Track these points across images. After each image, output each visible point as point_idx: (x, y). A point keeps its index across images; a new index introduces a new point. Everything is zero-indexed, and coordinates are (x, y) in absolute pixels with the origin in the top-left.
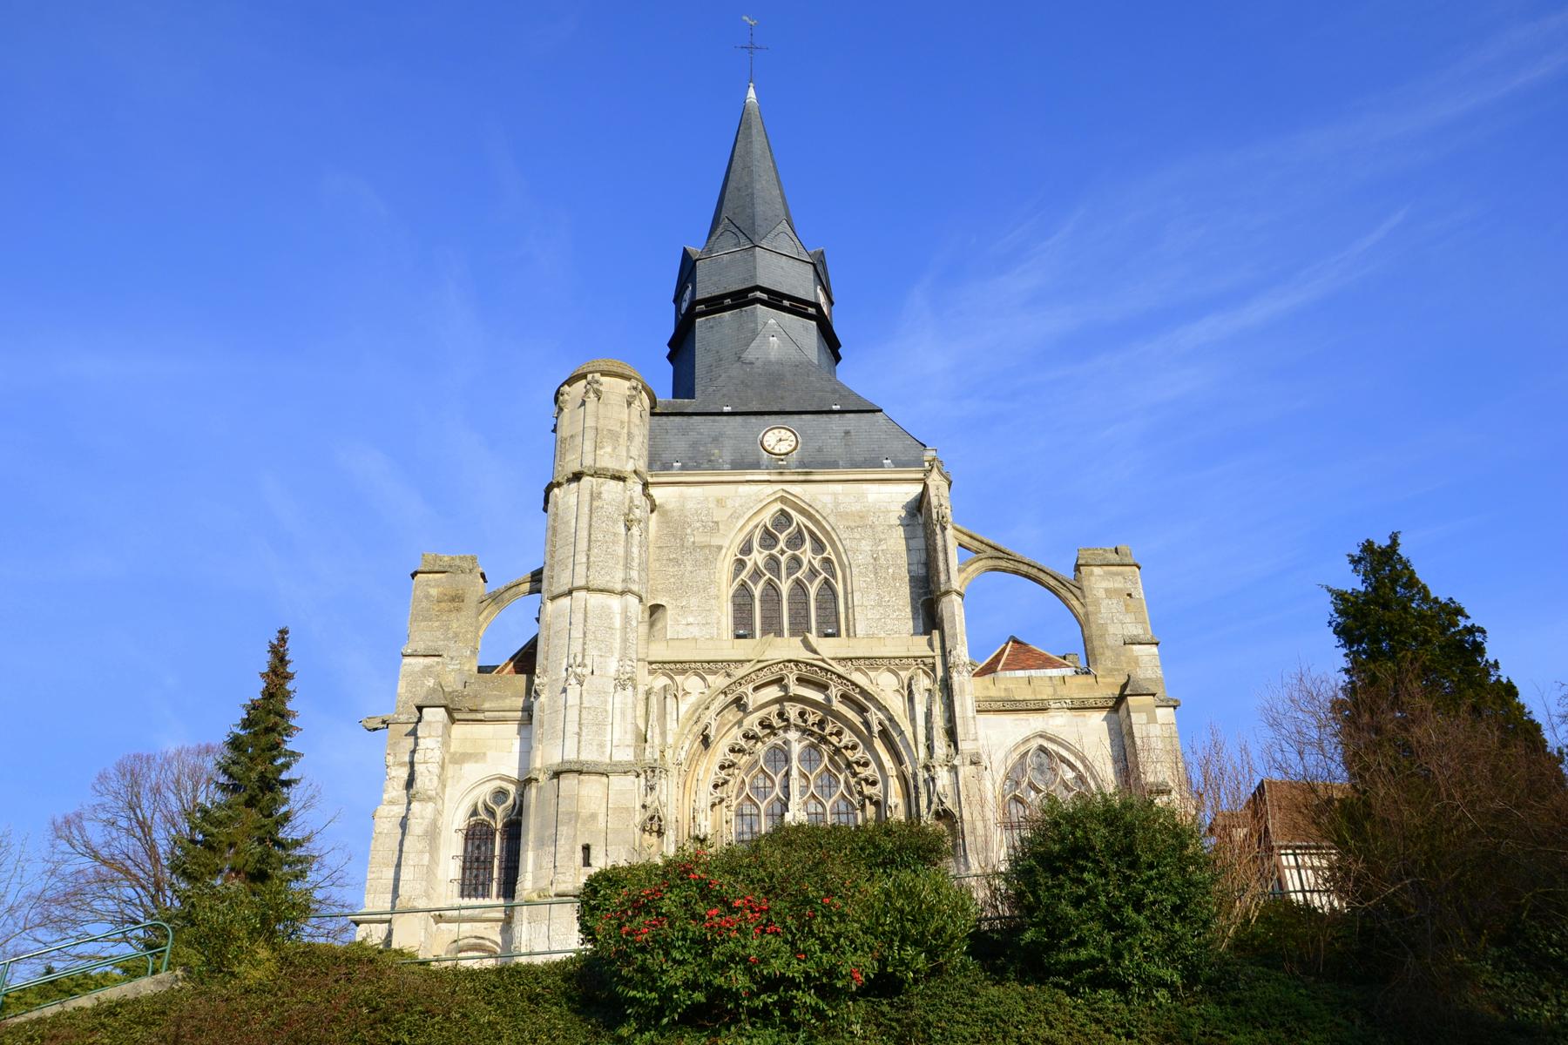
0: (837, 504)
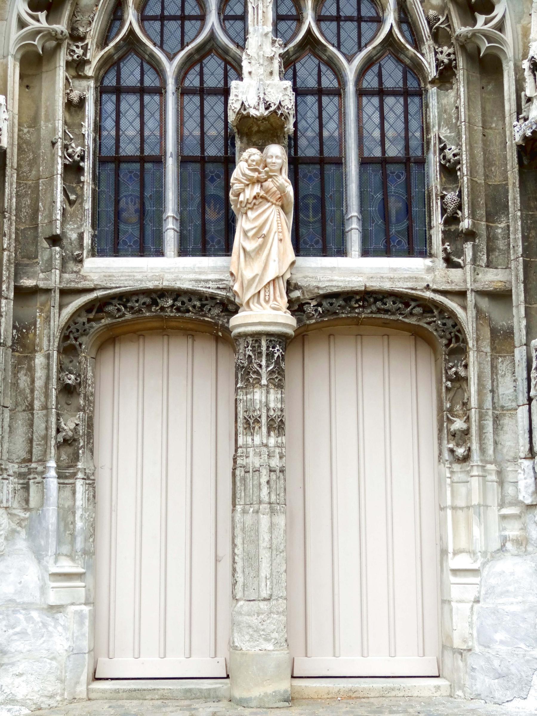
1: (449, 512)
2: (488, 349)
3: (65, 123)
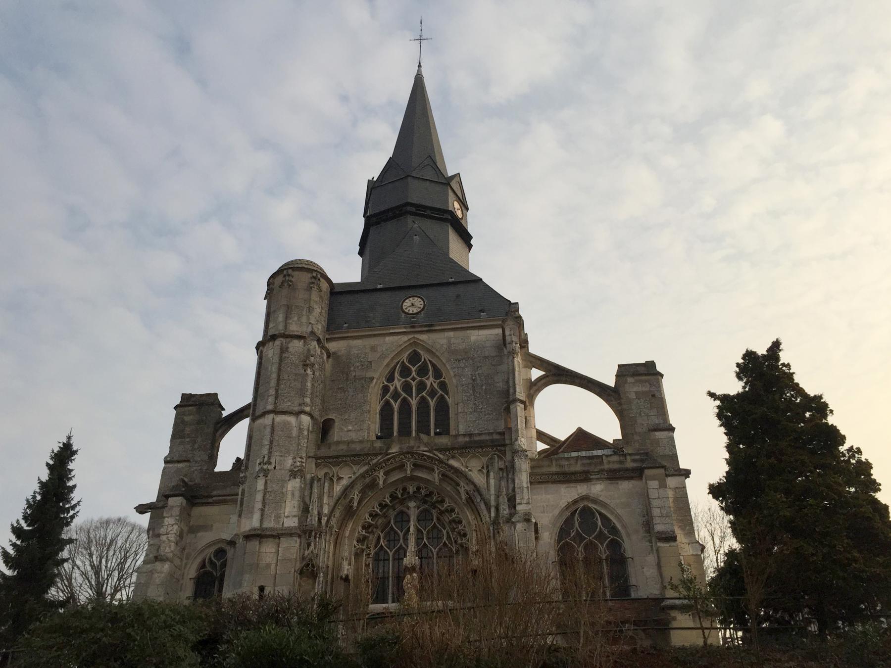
0: (449, 344)
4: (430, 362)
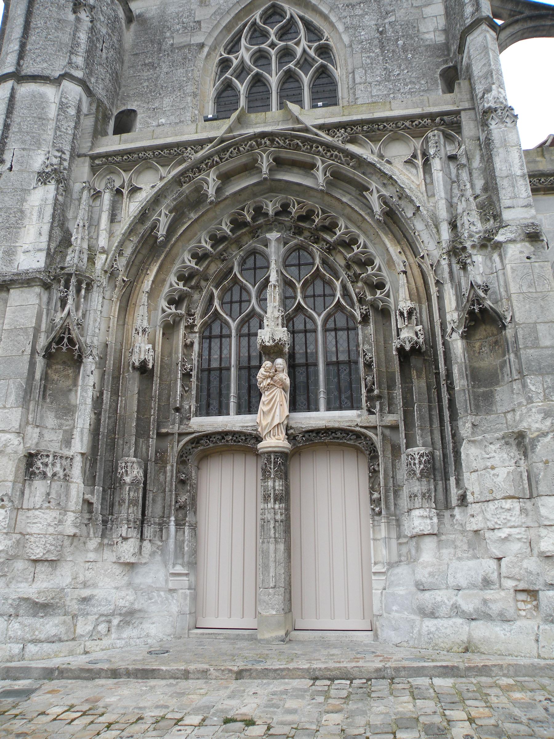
1: (372, 542)
2: (390, 456)
3: (184, 354)
4: (302, 18)
